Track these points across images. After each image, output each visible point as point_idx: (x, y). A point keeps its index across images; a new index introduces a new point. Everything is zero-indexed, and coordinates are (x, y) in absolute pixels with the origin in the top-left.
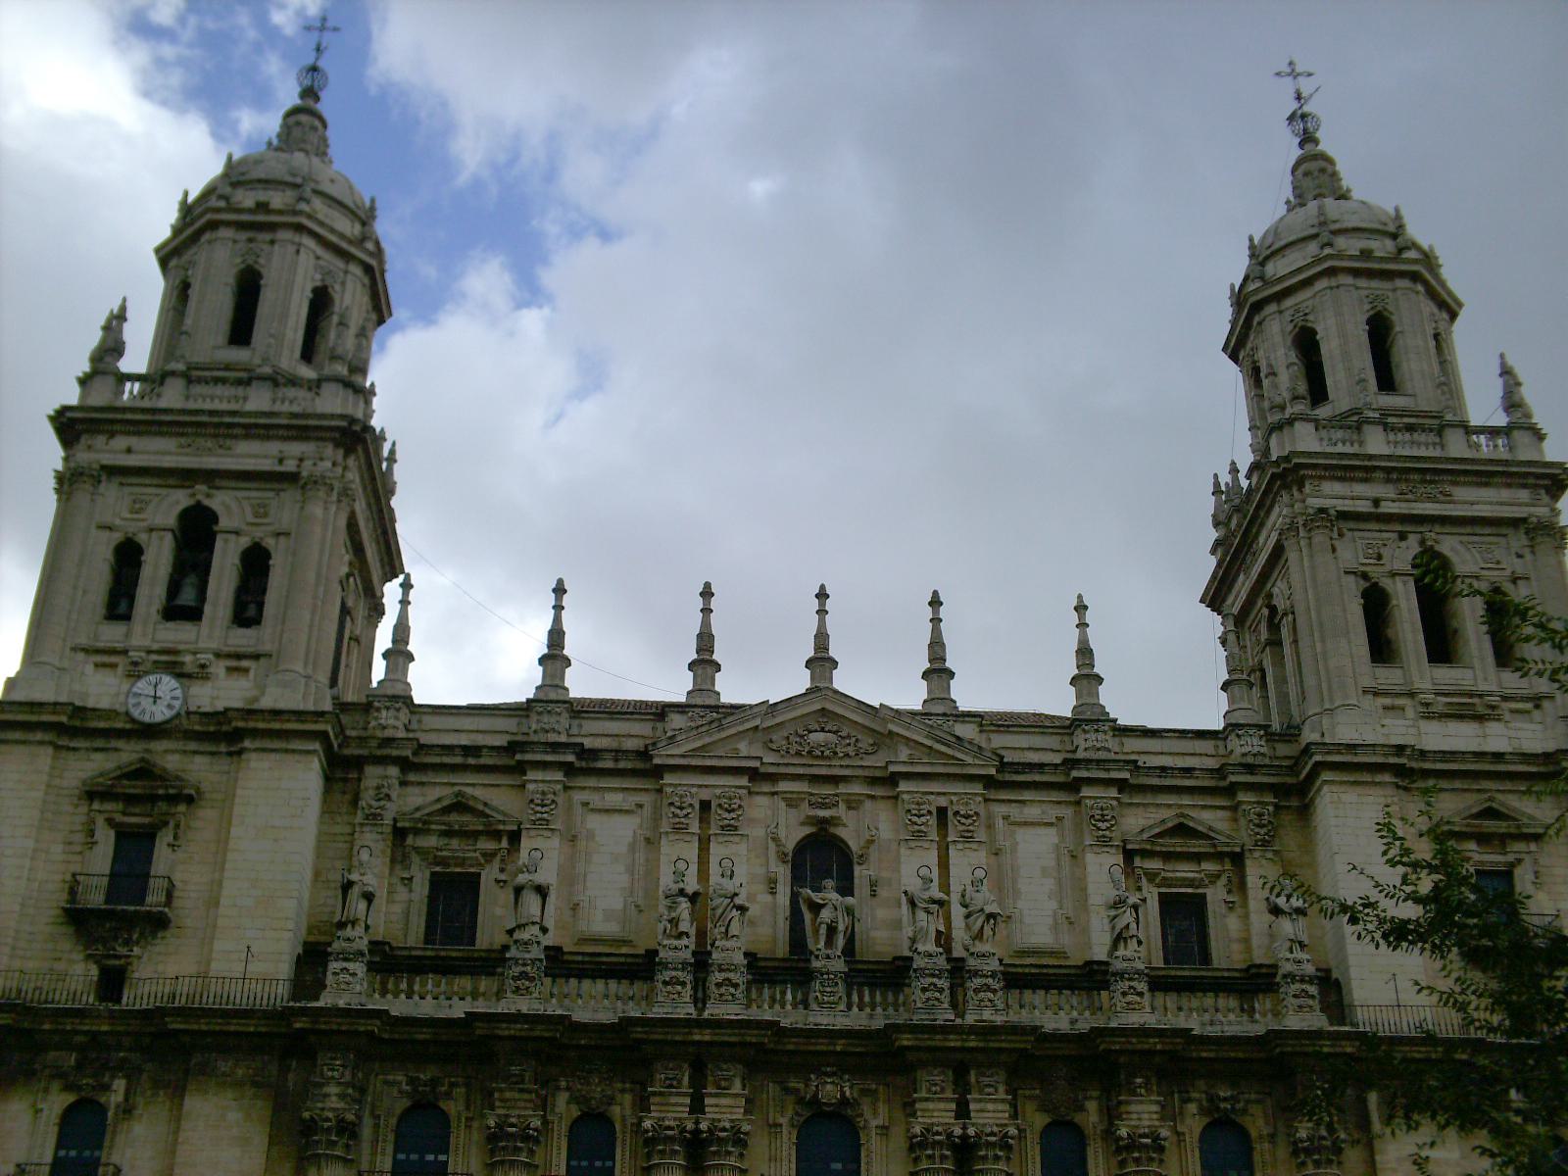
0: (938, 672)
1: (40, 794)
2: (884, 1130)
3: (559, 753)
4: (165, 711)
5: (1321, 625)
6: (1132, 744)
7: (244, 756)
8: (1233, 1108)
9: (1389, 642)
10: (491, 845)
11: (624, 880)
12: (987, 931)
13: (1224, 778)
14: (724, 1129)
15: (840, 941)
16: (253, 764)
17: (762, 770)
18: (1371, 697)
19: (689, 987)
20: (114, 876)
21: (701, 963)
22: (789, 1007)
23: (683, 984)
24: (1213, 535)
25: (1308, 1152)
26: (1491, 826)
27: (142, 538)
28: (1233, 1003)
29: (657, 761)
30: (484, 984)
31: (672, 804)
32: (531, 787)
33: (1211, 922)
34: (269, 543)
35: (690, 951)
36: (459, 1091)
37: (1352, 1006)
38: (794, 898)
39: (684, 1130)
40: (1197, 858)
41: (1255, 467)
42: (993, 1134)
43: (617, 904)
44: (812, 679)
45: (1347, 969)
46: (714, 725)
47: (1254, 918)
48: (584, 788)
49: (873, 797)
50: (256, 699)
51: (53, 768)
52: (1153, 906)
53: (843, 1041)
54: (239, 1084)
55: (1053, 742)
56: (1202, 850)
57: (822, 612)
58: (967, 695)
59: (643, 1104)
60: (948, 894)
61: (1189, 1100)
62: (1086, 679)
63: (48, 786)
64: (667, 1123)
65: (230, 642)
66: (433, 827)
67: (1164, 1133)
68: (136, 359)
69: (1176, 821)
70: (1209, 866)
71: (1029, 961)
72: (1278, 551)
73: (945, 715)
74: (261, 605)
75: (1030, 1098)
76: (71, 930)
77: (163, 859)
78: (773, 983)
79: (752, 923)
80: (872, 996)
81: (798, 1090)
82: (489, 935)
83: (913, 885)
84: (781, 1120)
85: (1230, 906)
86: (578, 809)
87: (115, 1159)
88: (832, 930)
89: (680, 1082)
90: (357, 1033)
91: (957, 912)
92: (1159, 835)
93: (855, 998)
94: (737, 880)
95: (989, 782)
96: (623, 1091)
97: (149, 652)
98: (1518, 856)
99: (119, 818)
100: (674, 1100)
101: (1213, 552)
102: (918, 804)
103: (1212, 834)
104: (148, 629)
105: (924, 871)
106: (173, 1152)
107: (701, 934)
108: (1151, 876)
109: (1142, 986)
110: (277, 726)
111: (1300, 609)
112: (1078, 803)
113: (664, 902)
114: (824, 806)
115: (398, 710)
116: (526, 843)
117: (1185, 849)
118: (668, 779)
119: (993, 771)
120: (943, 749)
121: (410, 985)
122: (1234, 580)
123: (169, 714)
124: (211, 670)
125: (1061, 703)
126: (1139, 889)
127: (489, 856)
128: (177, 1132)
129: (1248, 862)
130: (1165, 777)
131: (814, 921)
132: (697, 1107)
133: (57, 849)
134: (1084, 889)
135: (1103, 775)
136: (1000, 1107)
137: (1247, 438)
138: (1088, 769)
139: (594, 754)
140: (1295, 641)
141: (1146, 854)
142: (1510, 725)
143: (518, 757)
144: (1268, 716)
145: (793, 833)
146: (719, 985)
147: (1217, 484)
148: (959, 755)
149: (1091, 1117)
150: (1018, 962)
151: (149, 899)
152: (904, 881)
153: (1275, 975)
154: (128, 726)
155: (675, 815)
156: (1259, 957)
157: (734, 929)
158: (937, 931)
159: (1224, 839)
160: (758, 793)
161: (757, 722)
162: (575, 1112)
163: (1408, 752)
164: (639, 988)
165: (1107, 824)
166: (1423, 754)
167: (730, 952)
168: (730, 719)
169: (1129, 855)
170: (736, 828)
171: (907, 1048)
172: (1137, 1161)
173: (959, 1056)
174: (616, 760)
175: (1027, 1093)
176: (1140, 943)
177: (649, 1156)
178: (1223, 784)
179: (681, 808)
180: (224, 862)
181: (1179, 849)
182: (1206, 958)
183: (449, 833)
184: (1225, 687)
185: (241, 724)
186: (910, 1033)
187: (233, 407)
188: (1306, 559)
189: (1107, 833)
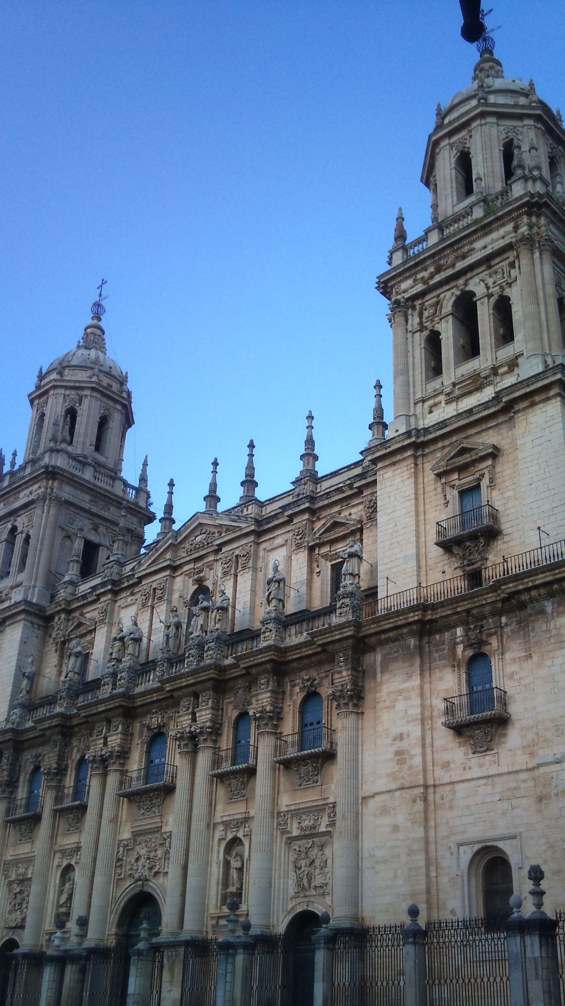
3: (105, 586)
8: (312, 685)
18: (420, 404)
26: (466, 458)
40: (344, 538)
46: (154, 550)
48: (121, 599)
53: (155, 695)
56: (344, 533)
57: (215, 472)
61: (295, 685)
66: (72, 636)
69: (332, 521)
75: (230, 703)
89: (102, 731)
98: (481, 473)
103: (347, 522)
108: (326, 557)
110: (10, 613)
115: (66, 588)
117: (336, 536)
119: (253, 528)
130: (330, 497)
135: (297, 509)
138: (291, 509)
148: (241, 525)
159: (352, 523)
160: (177, 576)
165: (300, 536)
168: (159, 545)
174: (128, 581)
175: (228, 700)
179: (145, 595)
181: (333, 537)
186: (168, 683)
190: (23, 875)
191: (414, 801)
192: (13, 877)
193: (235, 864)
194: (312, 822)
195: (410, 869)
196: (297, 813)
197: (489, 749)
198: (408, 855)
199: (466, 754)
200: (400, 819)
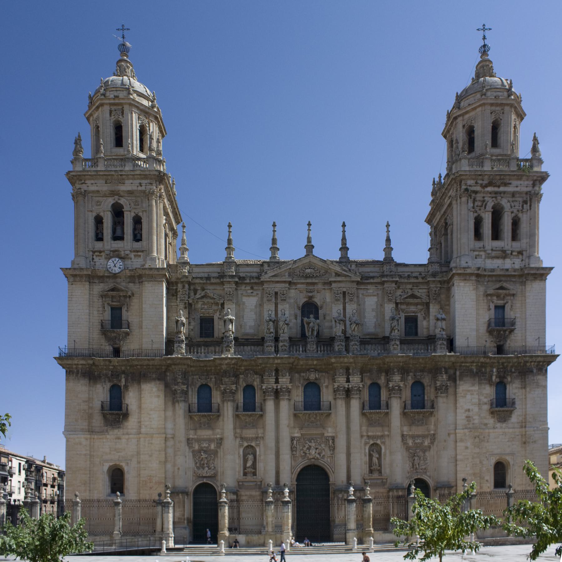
0: (344, 249)
1: (88, 296)
2: (327, 387)
4: (119, 269)
5: (460, 228)
6: (400, 269)
7: (143, 283)
9: (480, 234)
10: (215, 307)
11: (254, 316)
12: (356, 329)
13: (426, 279)
14: (284, 388)
15: (315, 333)
16: (146, 285)
17: (292, 282)
18: (472, 252)
19: (273, 347)
20: (112, 320)
21: (277, 339)
22: (301, 352)
23: (272, 347)
24: (431, 198)
25: (439, 390)
27: (102, 214)
28: (423, 347)
29: (262, 280)
30: (217, 349)
31: (267, 293)
32: (226, 289)
33: (419, 323)
34: (140, 214)
35: (273, 337)
36: (213, 380)
37: (455, 347)
38: (302, 321)
39: (274, 389)
41: (447, 175)
42: (356, 387)
43: (253, 324)
44: (307, 252)
45: (455, 336)
46: (278, 268)
47: (431, 321)
49: (324, 289)
50: (144, 265)
51: (90, 288)
52: (403, 319)
54: (154, 379)
55: (377, 269)
58: (353, 256)
59: (262, 382)
60: (345, 318)
62: (388, 249)
63: (90, 294)
64: (269, 387)
65: (134, 247)
67: (401, 385)
68: (87, 153)
70: (420, 307)
71: (368, 337)
72: (450, 205)
73: (346, 262)
74: (141, 235)
76: (103, 336)
77: (125, 314)
78: (296, 346)
79: (290, 328)
80: (324, 348)
81: (303, 376)
82: (217, 333)
83: (335, 315)
84: (300, 385)
85: (425, 318)
86: (240, 296)
87: (126, 402)
88: (313, 330)
90: (184, 364)
91: (348, 323)
92: (406, 298)
93: (319, 349)
94: (286, 316)
95: (358, 283)
96: (257, 378)
97: (111, 251)
99: (111, 303)
100: (271, 380)
101: (430, 205)
102: (337, 291)
104: (108, 244)
105: (339, 311)
106: (141, 400)
107: (277, 332)
109: (398, 343)
111: (455, 223)
112: (384, 289)
113: (266, 324)
114: (311, 292)
116: (226, 306)
118: (266, 286)
119: (359, 280)
120: (345, 273)
121: (197, 350)
122: (436, 214)
123: (119, 270)
124: (130, 256)
125: (381, 257)
126: (399, 314)
127: (215, 311)
128: (141, 394)
129: (431, 304)
131: (308, 327)
132: (277, 382)
133: (95, 313)
134: (384, 315)
135: (391, 280)
136: (358, 379)
137: (445, 165)
139: (244, 278)
140: (452, 234)
141: (401, 303)
142: (513, 260)
143: (222, 280)
144: (441, 259)
145: (302, 300)
146: (282, 346)
147: (434, 181)
148: (349, 275)
149: (382, 381)
150: (364, 337)
151: (123, 327)
152: (333, 314)
153: (435, 338)
154: (109, 275)
155: (268, 297)
156: (431, 333)
157: (286, 330)
158: (342, 329)
161: (290, 266)
162: (245, 385)
163: (481, 269)
164: (260, 348)
166: (485, 270)
167: (284, 336)
168: (283, 266)
169: (397, 304)
170: (285, 300)
171: (334, 363)
172: (394, 394)
173: (347, 365)
176: (398, 331)
177: (265, 396)
178: (426, 281)
180: (142, 315)
182: (416, 334)
183: (204, 304)
184: (429, 250)
185: (141, 273)
187: (121, 169)
188: (459, 207)
189: (391, 298)
190: (207, 447)
191: (475, 438)
192: (197, 447)
193: (376, 455)
194: (421, 441)
195: (473, 464)
196: (413, 437)
197: (505, 421)
198: (472, 459)
199: (494, 421)
200: (469, 444)
